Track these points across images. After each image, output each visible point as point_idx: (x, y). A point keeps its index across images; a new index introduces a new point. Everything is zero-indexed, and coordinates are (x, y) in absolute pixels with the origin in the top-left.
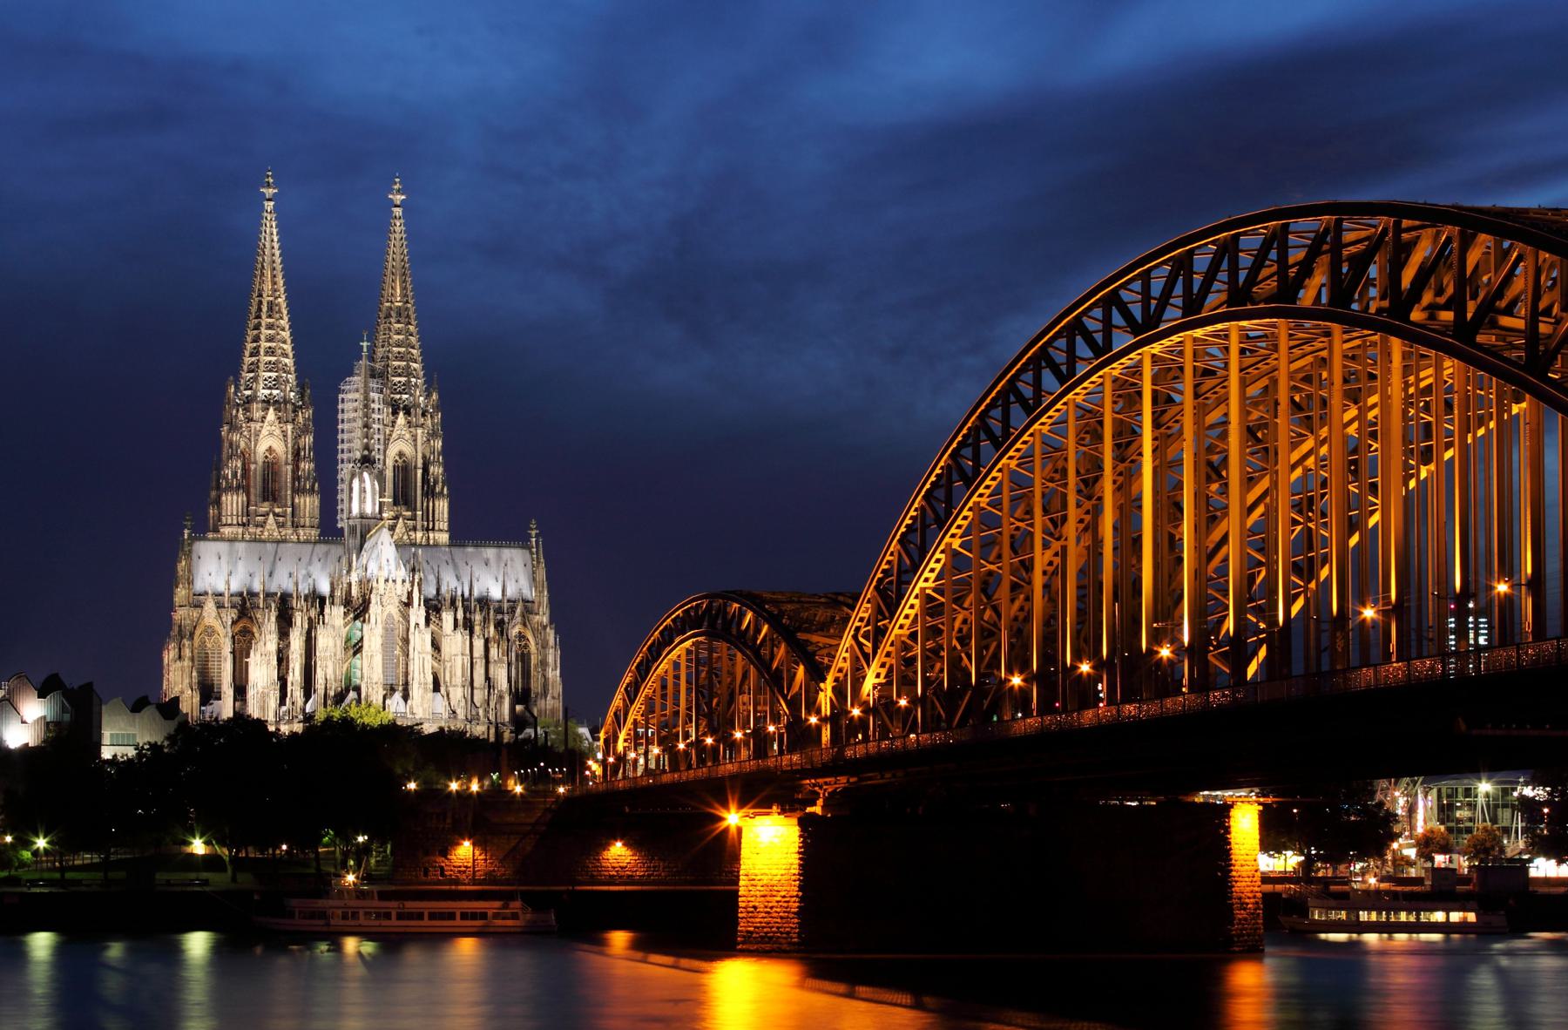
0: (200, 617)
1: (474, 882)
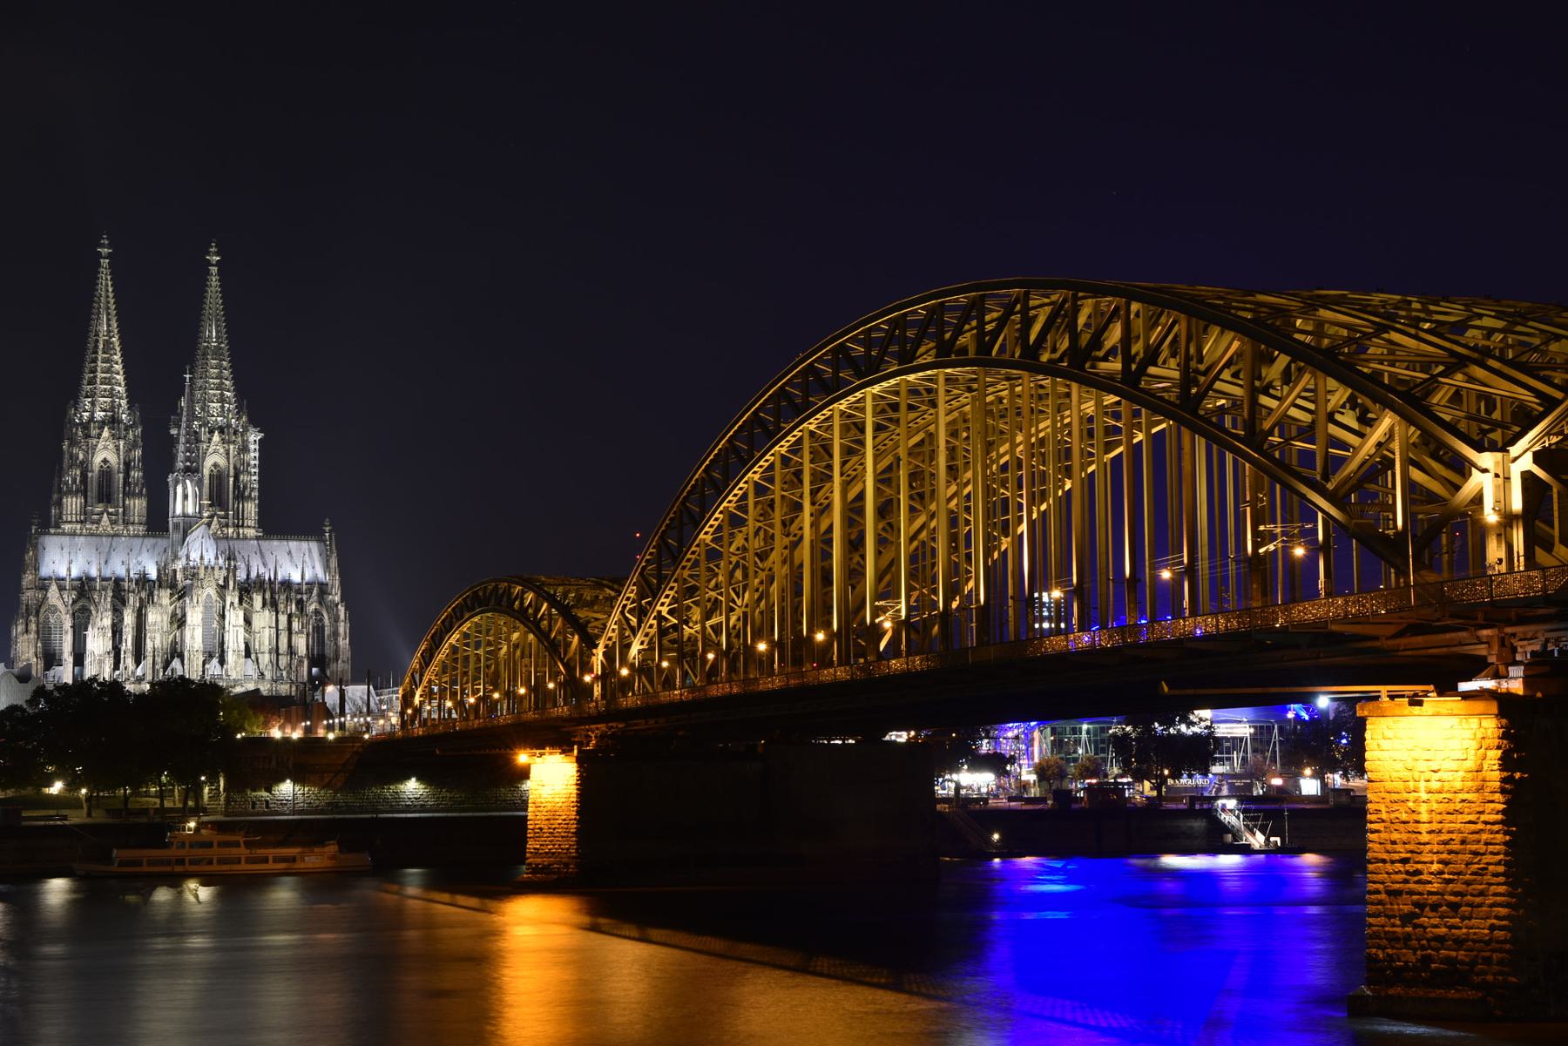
0: (45, 598)
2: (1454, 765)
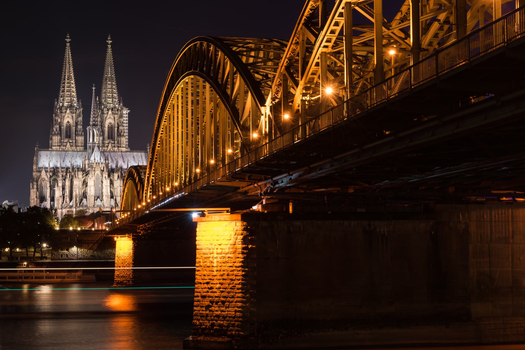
2: (226, 242)
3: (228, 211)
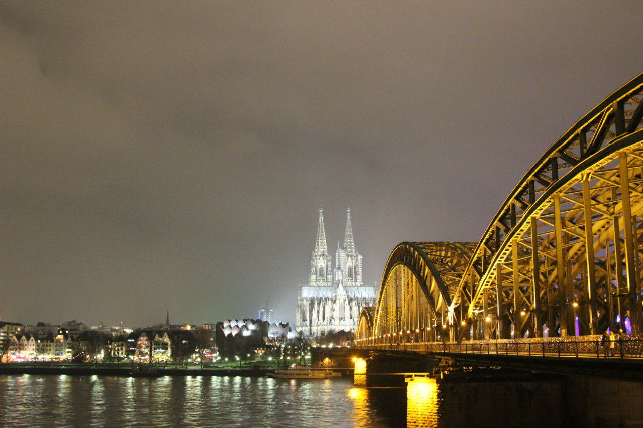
1: (329, 367)
3: (428, 376)
